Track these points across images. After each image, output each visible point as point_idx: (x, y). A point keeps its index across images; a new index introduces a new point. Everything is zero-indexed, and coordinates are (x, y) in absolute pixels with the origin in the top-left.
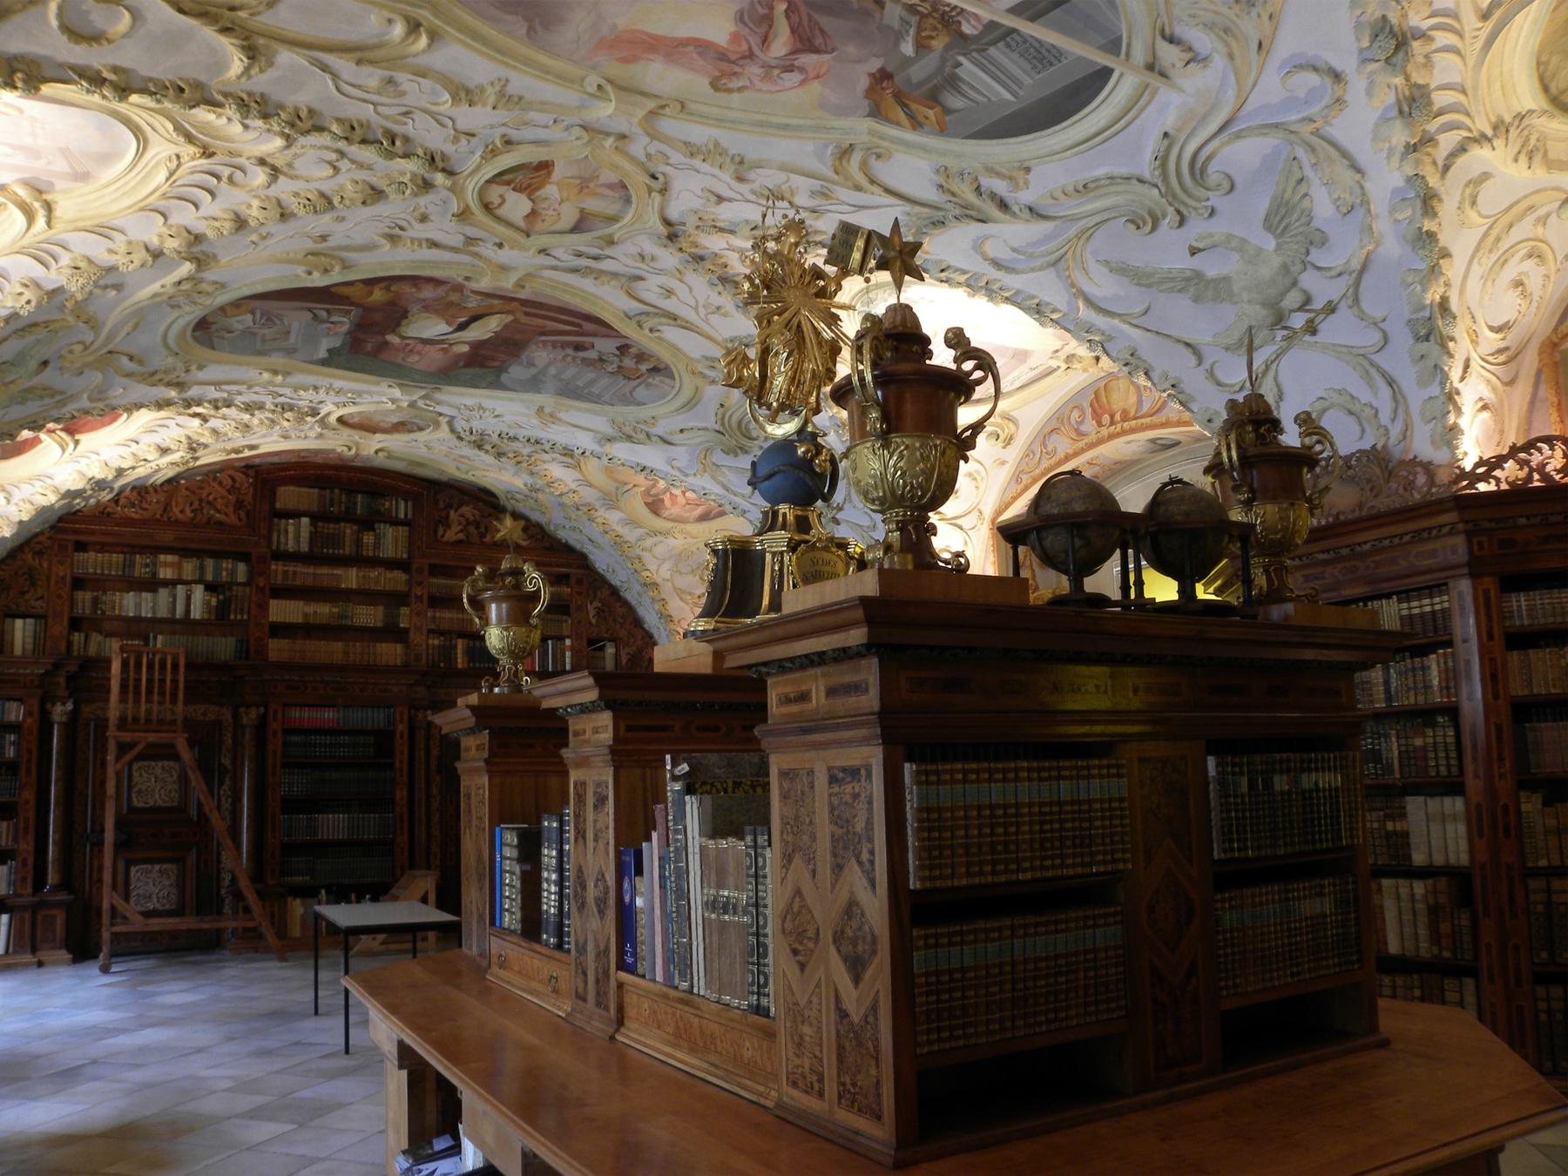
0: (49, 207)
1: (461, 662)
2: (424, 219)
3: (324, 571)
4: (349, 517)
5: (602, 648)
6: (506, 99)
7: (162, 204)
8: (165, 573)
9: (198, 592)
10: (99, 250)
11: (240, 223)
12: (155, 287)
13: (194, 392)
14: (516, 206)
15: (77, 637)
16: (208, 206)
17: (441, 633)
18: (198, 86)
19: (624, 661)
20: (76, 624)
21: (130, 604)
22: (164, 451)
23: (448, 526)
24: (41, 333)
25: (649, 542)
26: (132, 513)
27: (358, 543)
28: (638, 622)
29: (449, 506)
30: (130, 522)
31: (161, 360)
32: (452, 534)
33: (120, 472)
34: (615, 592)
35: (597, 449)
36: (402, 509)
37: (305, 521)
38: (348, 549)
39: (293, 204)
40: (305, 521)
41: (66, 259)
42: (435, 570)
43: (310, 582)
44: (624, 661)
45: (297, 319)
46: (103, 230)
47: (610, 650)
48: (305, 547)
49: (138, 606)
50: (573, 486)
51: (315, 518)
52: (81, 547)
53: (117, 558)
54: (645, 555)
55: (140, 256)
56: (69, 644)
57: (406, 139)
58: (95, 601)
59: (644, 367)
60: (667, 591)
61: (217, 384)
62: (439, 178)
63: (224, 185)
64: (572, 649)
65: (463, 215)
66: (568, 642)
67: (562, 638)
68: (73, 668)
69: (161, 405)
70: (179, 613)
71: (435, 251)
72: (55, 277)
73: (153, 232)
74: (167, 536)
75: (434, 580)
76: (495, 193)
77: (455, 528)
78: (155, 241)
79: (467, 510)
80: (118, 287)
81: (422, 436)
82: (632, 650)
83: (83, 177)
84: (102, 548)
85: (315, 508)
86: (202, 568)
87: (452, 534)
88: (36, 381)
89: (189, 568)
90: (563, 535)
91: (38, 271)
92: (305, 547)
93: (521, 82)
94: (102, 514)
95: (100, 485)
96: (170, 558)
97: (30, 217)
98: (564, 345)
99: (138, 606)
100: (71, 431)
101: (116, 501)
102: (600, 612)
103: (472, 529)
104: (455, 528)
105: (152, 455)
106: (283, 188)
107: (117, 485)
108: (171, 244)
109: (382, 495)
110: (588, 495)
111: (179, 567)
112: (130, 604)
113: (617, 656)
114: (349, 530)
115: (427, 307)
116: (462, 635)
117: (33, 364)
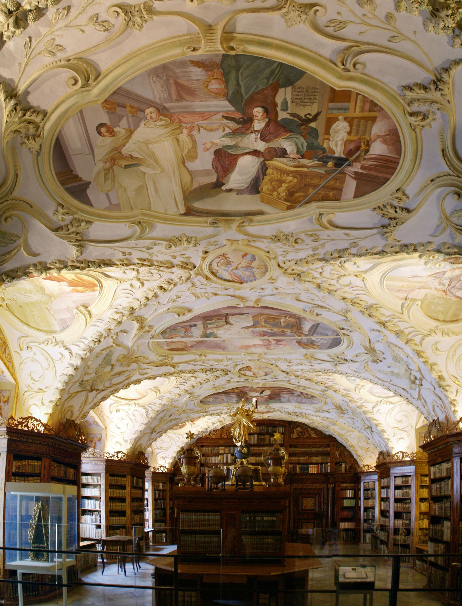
0: (159, 390)
1: (298, 471)
2: (232, 378)
3: (261, 448)
4: (267, 433)
5: (341, 465)
6: (228, 359)
7: (179, 386)
8: (221, 452)
9: (229, 456)
10: (170, 396)
11: (194, 387)
12: (185, 399)
13: (211, 412)
14: (248, 373)
15: (202, 468)
16: (186, 385)
17: (292, 463)
18: (168, 373)
19: (348, 468)
20: (202, 465)
21: (214, 460)
22: (214, 423)
23: (293, 434)
24: (166, 411)
25: (349, 434)
26: (213, 437)
27: (270, 440)
28: (352, 456)
29: (294, 428)
30: (213, 439)
31: (197, 409)
32: (295, 436)
33: (207, 429)
34: (345, 447)
35: (314, 413)
36: (281, 430)
37: (256, 435)
38: (267, 442)
39: (202, 382)
40: (256, 435)
41: (165, 399)
42: (291, 446)
43: (257, 452)
44: (348, 468)
45: (223, 397)
46: (170, 392)
47: (343, 465)
48: (256, 443)
49: (215, 460)
50: (321, 421)
51: (258, 434)
52: (203, 446)
53: (210, 448)
54: (348, 438)
55: (177, 396)
56: (200, 470)
57: (215, 369)
58: (206, 459)
59: (310, 396)
60: (357, 448)
61: (216, 410)
62: (228, 372)
63: (187, 381)
64: (330, 466)
65: (239, 376)
66: (329, 464)
67: (327, 463)
68: (201, 476)
69: (204, 416)
70: (225, 461)
71: (239, 383)
72: (164, 402)
73: (178, 391)
74: (222, 442)
75: (290, 449)
76: (242, 372)
77: (295, 434)
78: (179, 393)
79: (299, 429)
80: (177, 401)
81: (275, 413)
82: (350, 465)
83: (163, 384)
84: (208, 446)
85: (258, 432)
86: (230, 450)
87: (295, 436)
88: (171, 418)
89: (227, 450)
90: (327, 433)
91: (161, 402)
92: (256, 443)
93: (229, 357)
94: (206, 438)
95: (203, 432)
96: (222, 448)
97: (157, 393)
98: (288, 394)
99: (215, 460)
100: (192, 421)
101: (209, 434)
102: (340, 454)
103: (300, 434)
104: (295, 434)
105: (211, 425)
106: (198, 379)
107: (208, 431)
108: (182, 393)
109: (276, 427)
110: (326, 423)
111: (224, 450)
112: (214, 460)
113: (346, 467)
114: (267, 437)
115: (250, 391)
116: (298, 464)
117: (168, 417)
